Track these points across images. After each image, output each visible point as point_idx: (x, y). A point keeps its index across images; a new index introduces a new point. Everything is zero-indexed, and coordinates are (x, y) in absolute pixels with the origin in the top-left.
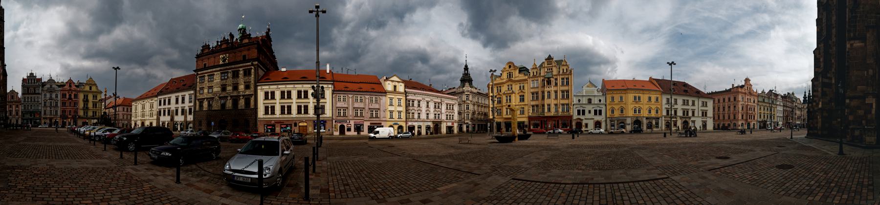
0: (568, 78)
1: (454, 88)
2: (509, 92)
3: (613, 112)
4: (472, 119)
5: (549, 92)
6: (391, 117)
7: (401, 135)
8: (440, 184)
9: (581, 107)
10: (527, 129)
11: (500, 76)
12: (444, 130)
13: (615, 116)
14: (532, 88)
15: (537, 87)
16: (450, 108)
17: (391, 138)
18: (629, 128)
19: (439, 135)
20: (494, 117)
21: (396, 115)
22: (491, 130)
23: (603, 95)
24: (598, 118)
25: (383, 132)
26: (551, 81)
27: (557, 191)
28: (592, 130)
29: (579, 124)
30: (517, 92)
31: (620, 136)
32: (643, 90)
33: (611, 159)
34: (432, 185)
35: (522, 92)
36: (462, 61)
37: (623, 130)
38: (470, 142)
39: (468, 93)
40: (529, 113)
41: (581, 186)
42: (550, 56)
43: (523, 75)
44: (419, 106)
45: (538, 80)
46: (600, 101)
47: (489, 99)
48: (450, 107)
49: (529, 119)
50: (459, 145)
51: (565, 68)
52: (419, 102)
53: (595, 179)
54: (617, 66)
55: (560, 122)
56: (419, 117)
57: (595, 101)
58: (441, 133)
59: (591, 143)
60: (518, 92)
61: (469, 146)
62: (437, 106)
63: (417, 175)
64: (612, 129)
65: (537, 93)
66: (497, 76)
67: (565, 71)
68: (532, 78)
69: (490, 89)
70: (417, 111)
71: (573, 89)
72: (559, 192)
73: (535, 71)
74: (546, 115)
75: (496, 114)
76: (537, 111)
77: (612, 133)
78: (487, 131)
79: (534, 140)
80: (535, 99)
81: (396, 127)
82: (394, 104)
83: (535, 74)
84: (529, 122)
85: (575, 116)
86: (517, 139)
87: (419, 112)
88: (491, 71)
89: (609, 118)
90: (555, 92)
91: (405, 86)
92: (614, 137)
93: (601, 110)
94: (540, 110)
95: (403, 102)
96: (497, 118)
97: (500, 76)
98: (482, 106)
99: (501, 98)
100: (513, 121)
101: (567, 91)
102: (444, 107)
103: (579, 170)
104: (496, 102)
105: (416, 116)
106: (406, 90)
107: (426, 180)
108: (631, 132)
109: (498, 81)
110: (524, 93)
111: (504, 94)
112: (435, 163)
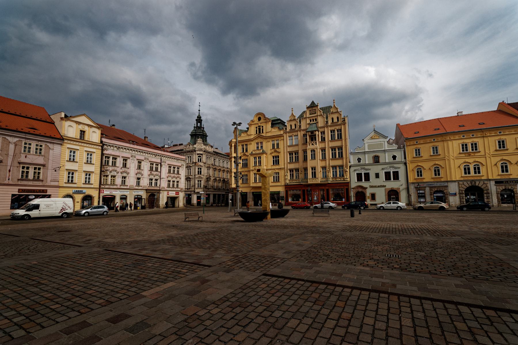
0: (341, 130)
1: (182, 144)
2: (258, 152)
3: (420, 173)
4: (205, 187)
5: (313, 151)
6: (71, 180)
7: (89, 210)
8: (147, 285)
9: (362, 169)
10: (283, 202)
11: (246, 132)
12: (163, 200)
13: (424, 181)
14: (289, 146)
15: (297, 145)
16: (174, 171)
17: (65, 216)
18: (454, 201)
19: (155, 209)
20: (237, 186)
21: (79, 179)
22: (234, 204)
23: (399, 148)
24: (392, 184)
25: (48, 206)
26: (315, 135)
27: (329, 297)
28: (382, 203)
29: (361, 195)
30: (269, 152)
31: (436, 215)
32: (481, 130)
33: (423, 254)
34: (134, 289)
35: (276, 151)
36: (194, 110)
37: (443, 205)
38: (201, 219)
39: (201, 152)
40: (285, 179)
41: (373, 294)
42: (313, 103)
43: (277, 130)
44: (125, 165)
45: (297, 135)
46: (394, 157)
47: (231, 161)
48: (173, 170)
49: (286, 188)
50: (184, 224)
51: (335, 116)
52: (125, 160)
53: (398, 286)
54: (422, 100)
55: (331, 192)
56: (124, 182)
57: (387, 158)
58: (158, 206)
59: (384, 224)
60: (270, 152)
61: (199, 225)
62: (155, 168)
63: (108, 276)
64: (420, 202)
65: (297, 153)
66: (242, 131)
67: (335, 120)
68: (289, 132)
69: (233, 148)
70: (121, 173)
71: (348, 144)
72: (333, 298)
73: (293, 123)
74: (310, 182)
75: (240, 181)
76: (298, 177)
77: (421, 209)
78: (227, 205)
79: (294, 217)
80: (294, 161)
81: (79, 198)
82: (77, 159)
83: (293, 127)
85: (354, 183)
86: (269, 216)
87: (125, 175)
88: (234, 124)
89: (413, 183)
90: (322, 150)
91: (102, 134)
92: (426, 215)
93: (397, 172)
94: (301, 176)
95: (96, 158)
96: (243, 187)
97: (246, 132)
98: (220, 170)
99: (247, 159)
100: (263, 191)
101: (340, 148)
102: (165, 170)
103: (364, 266)
104: (240, 166)
105: (118, 181)
106: (104, 140)
107: (124, 281)
108: (460, 208)
109: (244, 137)
110: (279, 152)
111: (252, 154)
112: (144, 253)
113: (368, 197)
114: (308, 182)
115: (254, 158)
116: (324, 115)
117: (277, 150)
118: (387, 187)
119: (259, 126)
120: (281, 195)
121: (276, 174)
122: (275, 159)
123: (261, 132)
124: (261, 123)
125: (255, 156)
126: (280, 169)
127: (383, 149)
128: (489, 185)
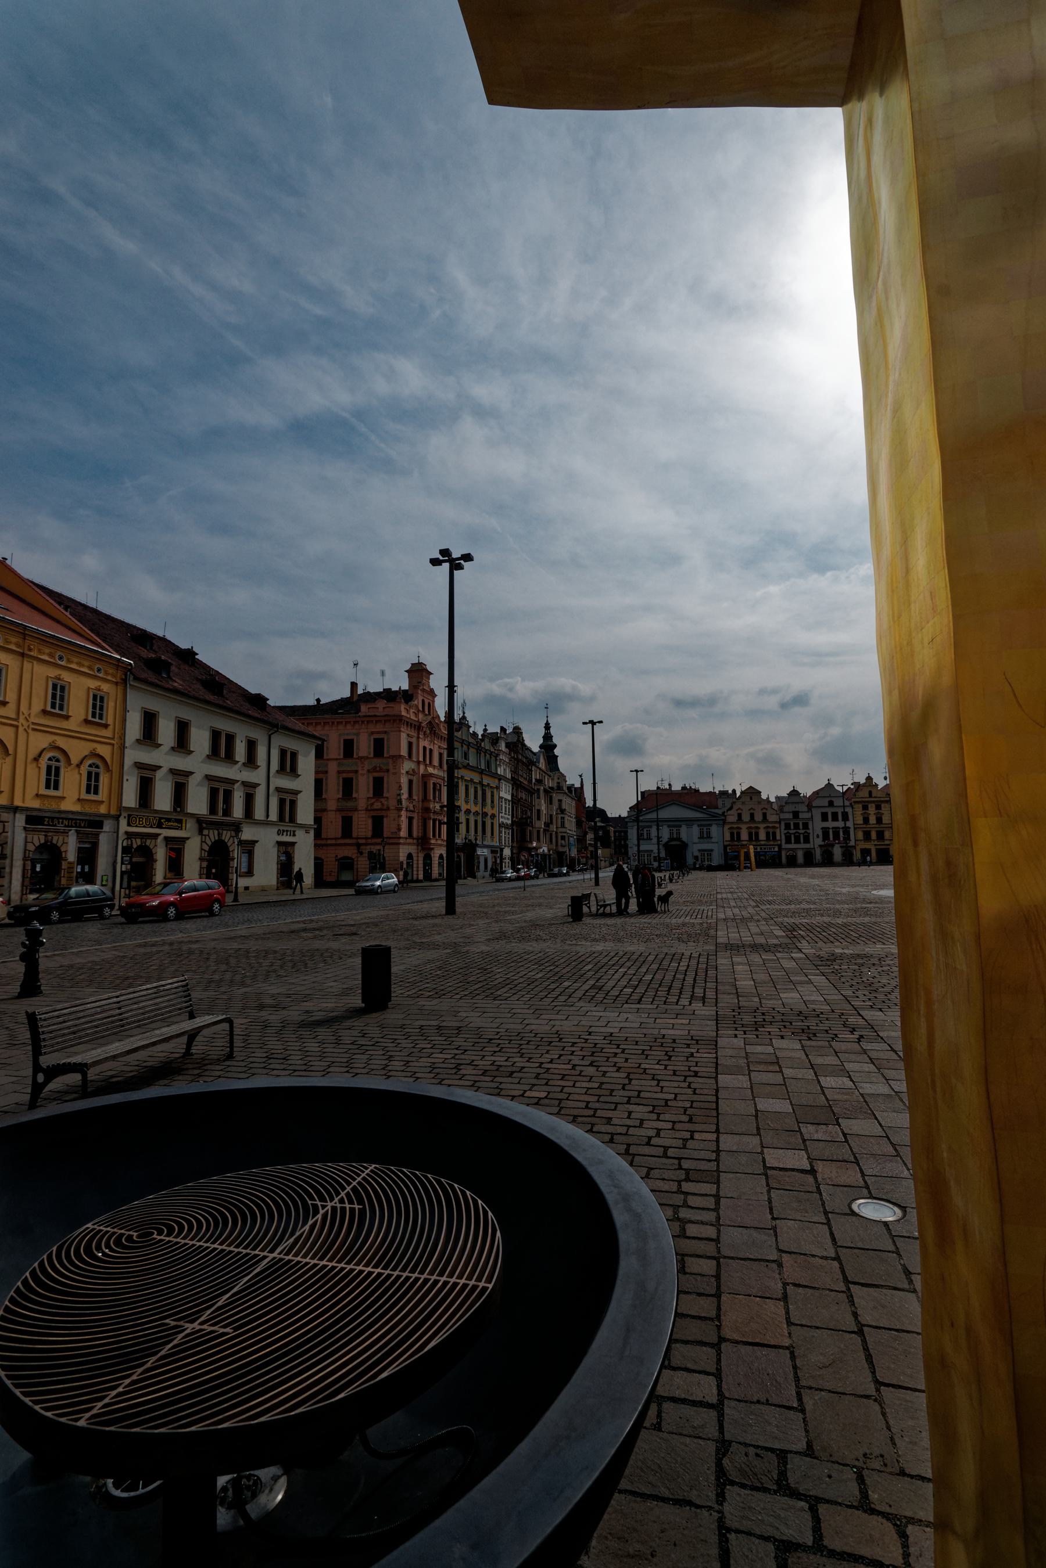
128: (9, 828)
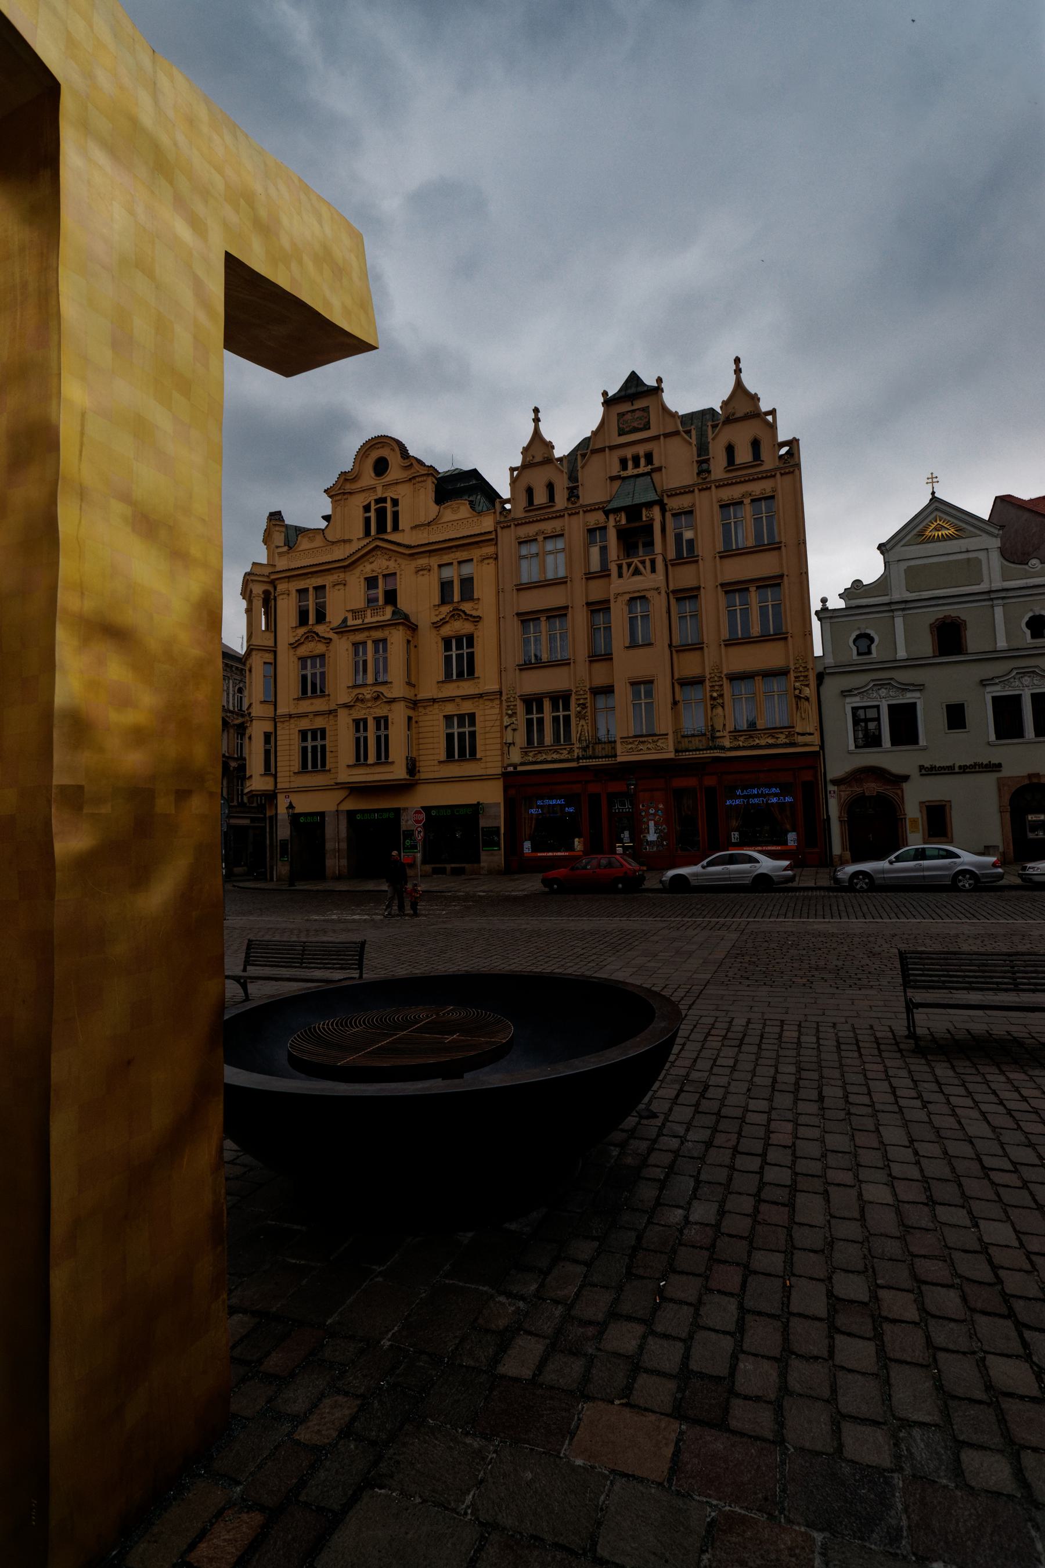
26: (649, 528)
35: (457, 614)
67: (743, 455)
84: (511, 804)
110: (477, 620)
111: (343, 629)
113: (914, 821)
114: (615, 756)
115: (356, 645)
116: (688, 432)
117: (467, 607)
118: (1006, 772)
119: (377, 501)
120: (483, 823)
121: (461, 725)
122: (454, 653)
123: (389, 529)
124: (386, 486)
125: (360, 637)
126: (481, 696)
127: (984, 587)
